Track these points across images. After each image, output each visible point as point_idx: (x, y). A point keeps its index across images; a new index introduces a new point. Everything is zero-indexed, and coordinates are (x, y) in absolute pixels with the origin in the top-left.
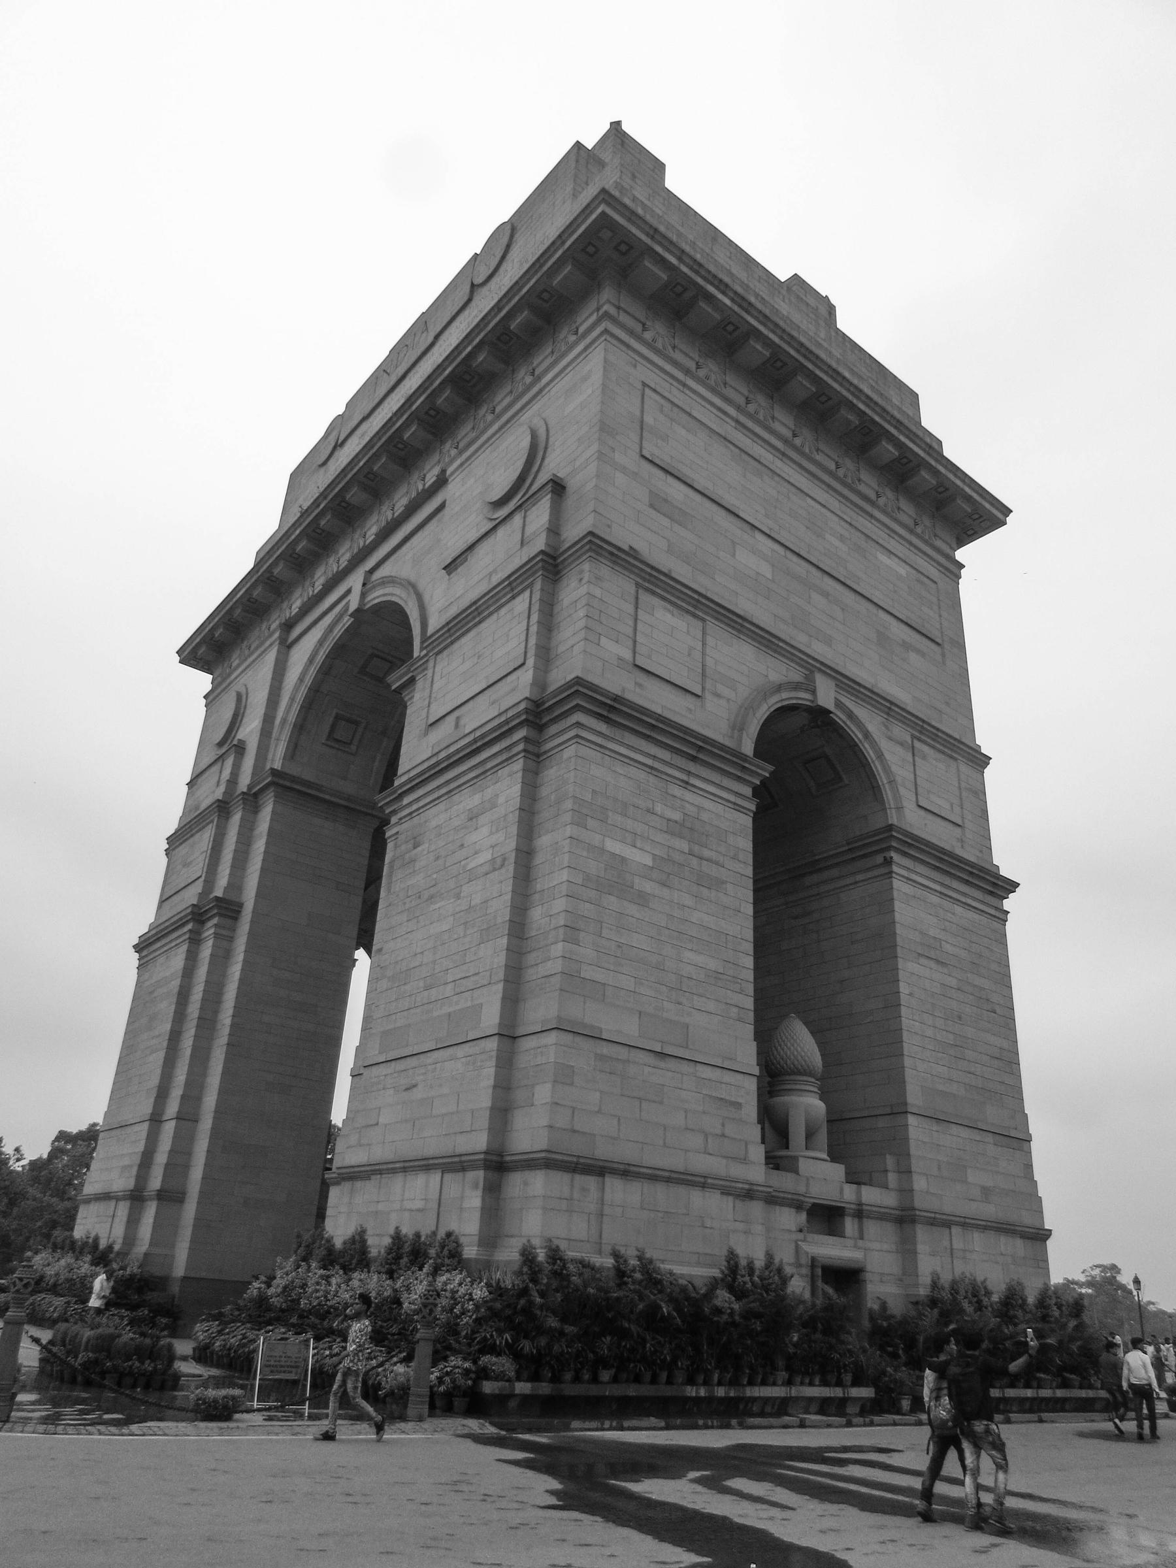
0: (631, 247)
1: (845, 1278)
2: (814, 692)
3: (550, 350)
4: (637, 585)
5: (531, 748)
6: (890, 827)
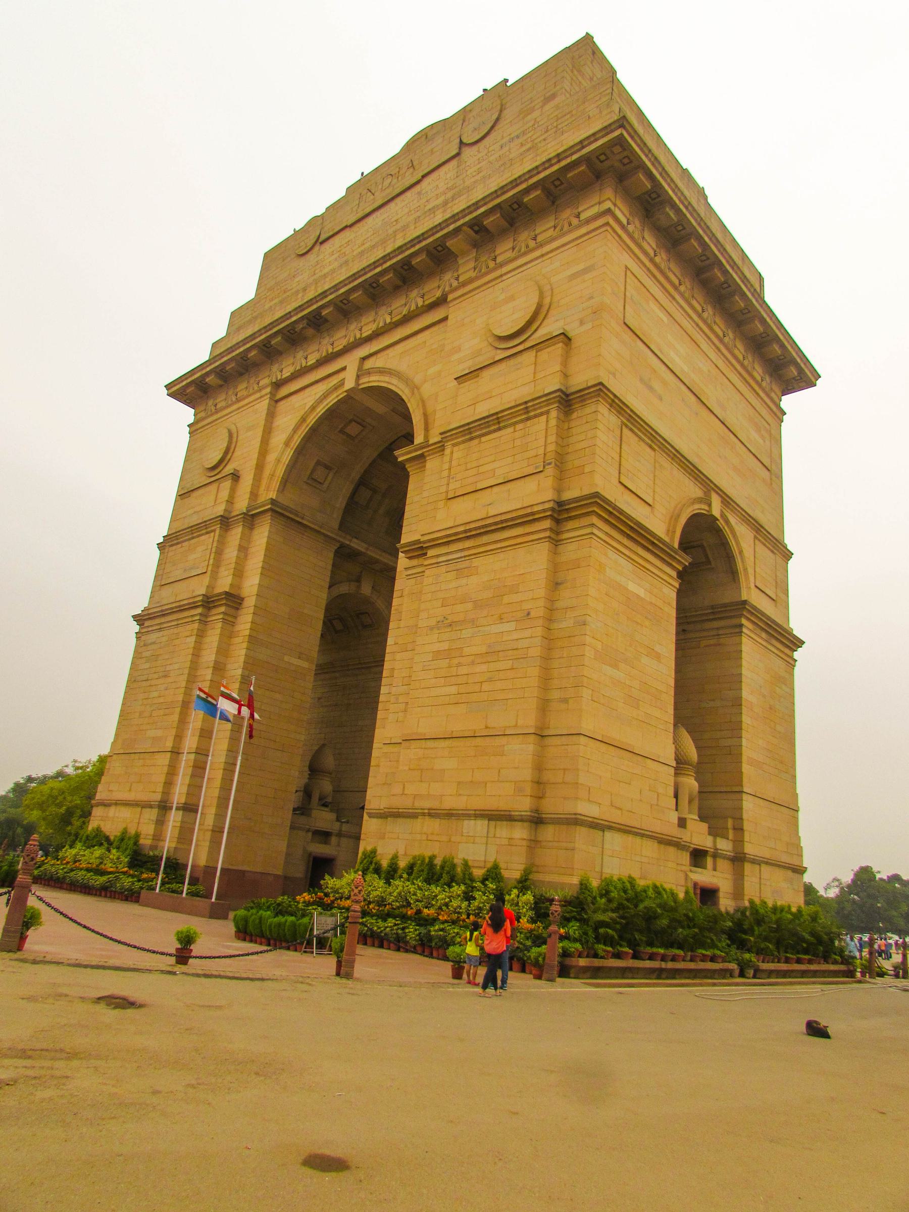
0: (631, 162)
1: (708, 894)
2: (710, 505)
3: (552, 224)
4: (622, 422)
5: (553, 536)
6: (745, 602)
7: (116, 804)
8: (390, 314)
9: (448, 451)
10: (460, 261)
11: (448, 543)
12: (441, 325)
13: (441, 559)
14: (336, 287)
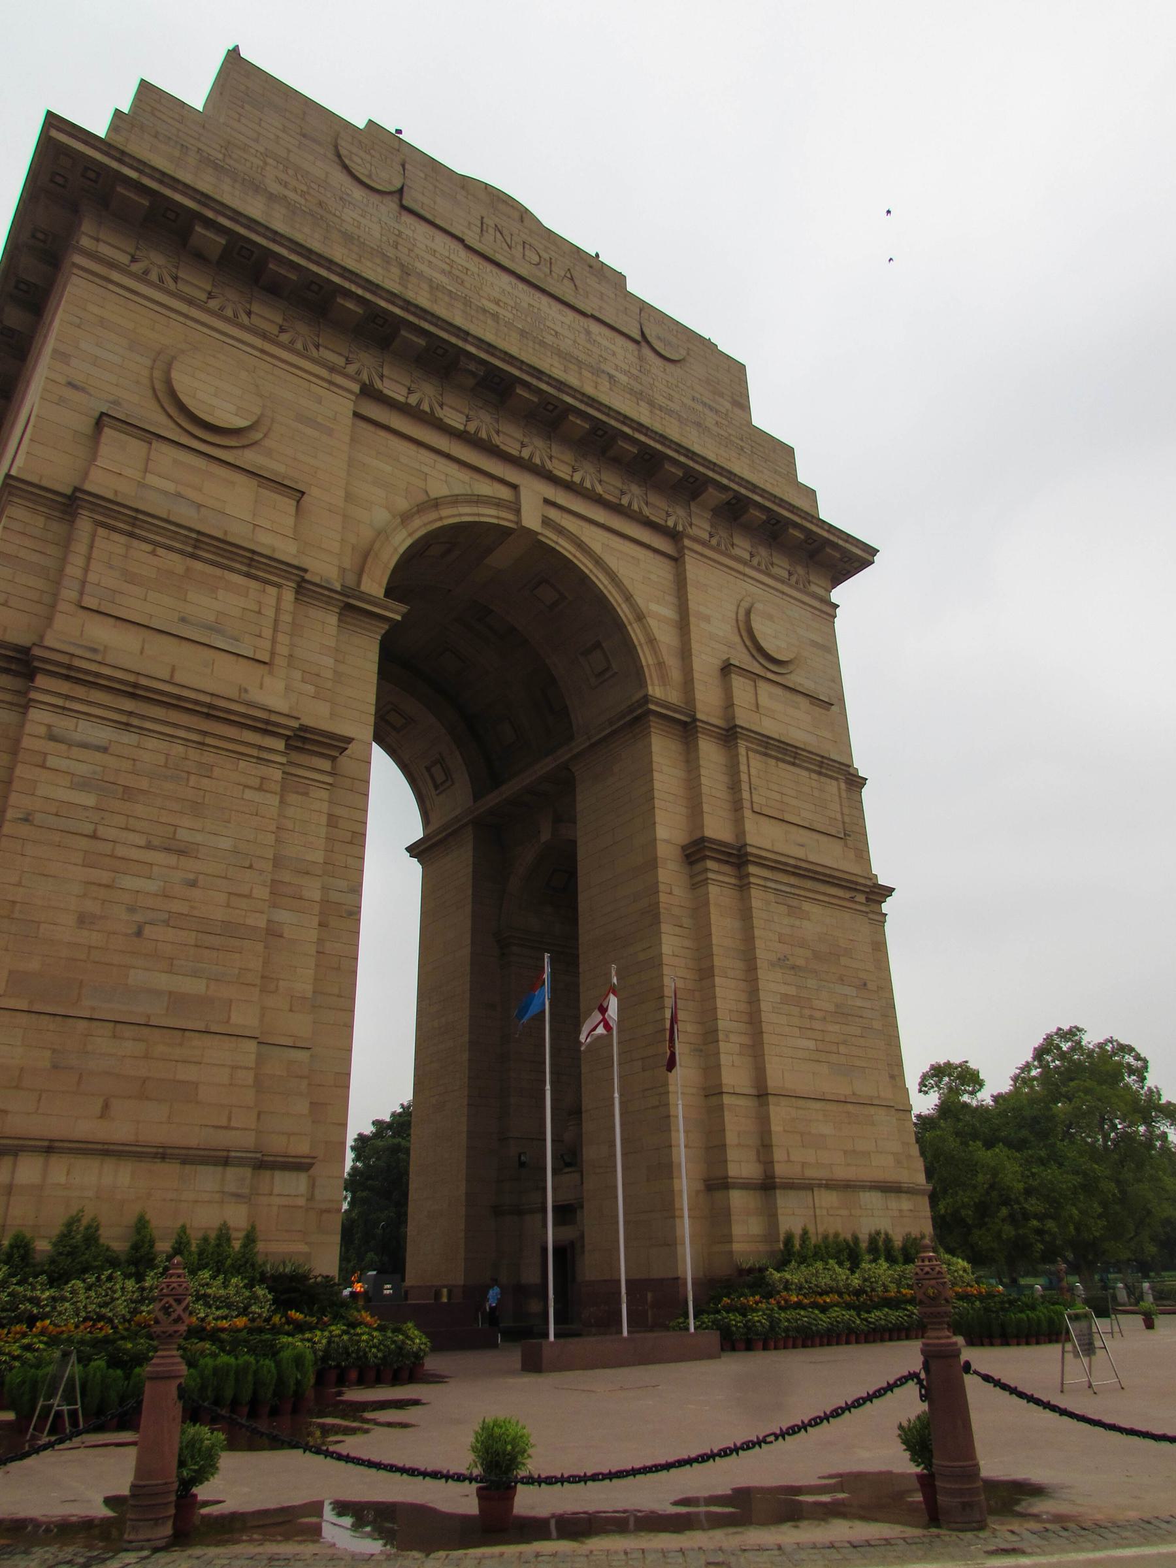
7: (50, 1148)
8: (600, 481)
9: (742, 751)
10: (694, 508)
11: (772, 868)
12: (659, 558)
13: (769, 884)
14: (561, 385)
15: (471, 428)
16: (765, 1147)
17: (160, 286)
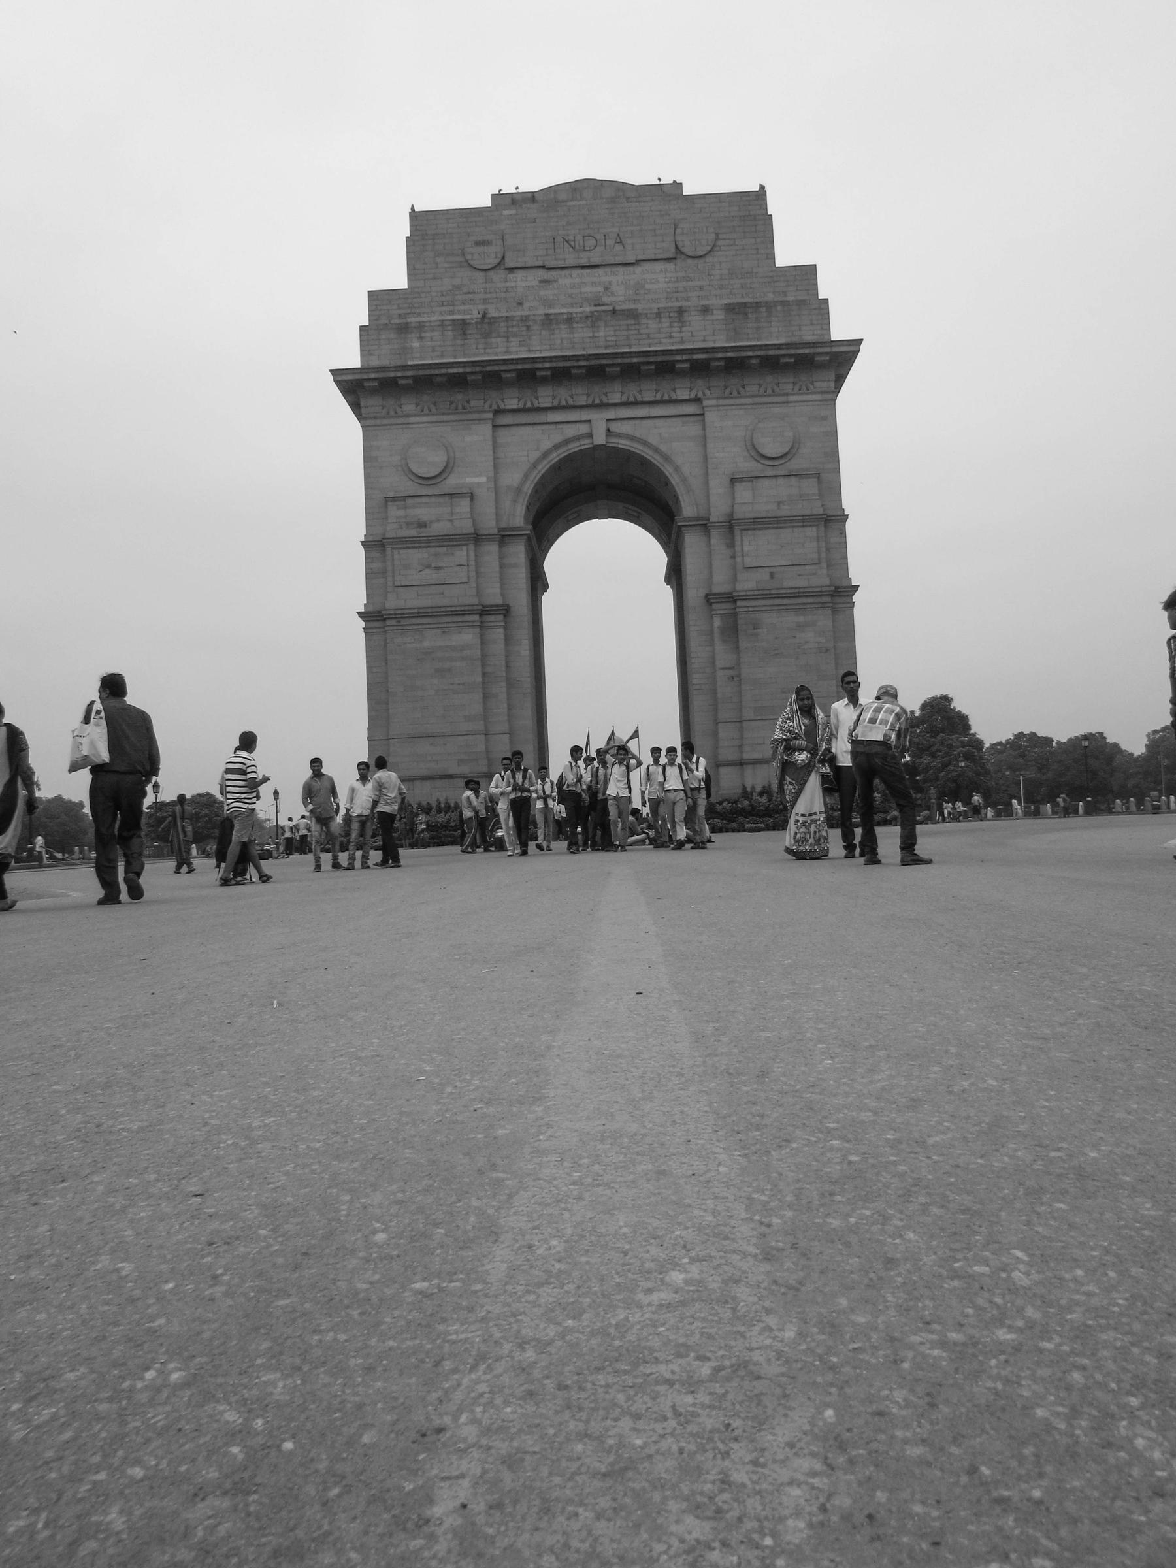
3: (792, 380)
9: (737, 532)
15: (556, 403)
16: (741, 746)
17: (396, 415)
